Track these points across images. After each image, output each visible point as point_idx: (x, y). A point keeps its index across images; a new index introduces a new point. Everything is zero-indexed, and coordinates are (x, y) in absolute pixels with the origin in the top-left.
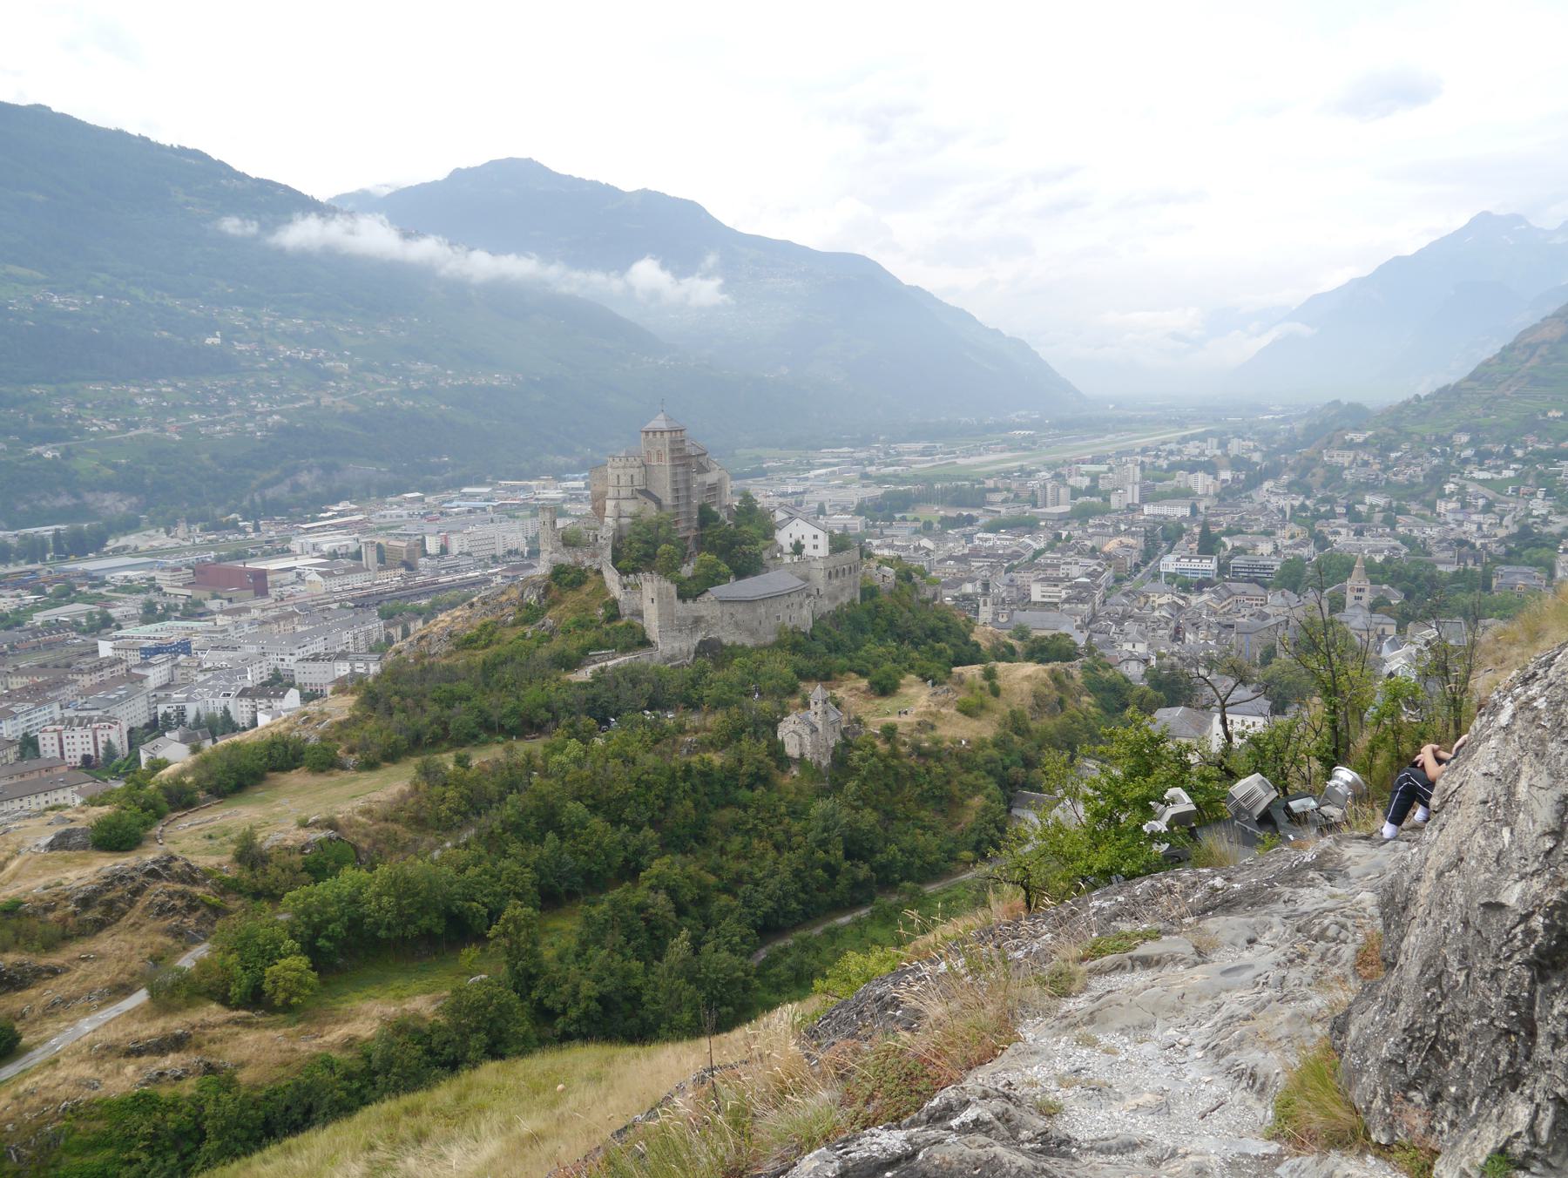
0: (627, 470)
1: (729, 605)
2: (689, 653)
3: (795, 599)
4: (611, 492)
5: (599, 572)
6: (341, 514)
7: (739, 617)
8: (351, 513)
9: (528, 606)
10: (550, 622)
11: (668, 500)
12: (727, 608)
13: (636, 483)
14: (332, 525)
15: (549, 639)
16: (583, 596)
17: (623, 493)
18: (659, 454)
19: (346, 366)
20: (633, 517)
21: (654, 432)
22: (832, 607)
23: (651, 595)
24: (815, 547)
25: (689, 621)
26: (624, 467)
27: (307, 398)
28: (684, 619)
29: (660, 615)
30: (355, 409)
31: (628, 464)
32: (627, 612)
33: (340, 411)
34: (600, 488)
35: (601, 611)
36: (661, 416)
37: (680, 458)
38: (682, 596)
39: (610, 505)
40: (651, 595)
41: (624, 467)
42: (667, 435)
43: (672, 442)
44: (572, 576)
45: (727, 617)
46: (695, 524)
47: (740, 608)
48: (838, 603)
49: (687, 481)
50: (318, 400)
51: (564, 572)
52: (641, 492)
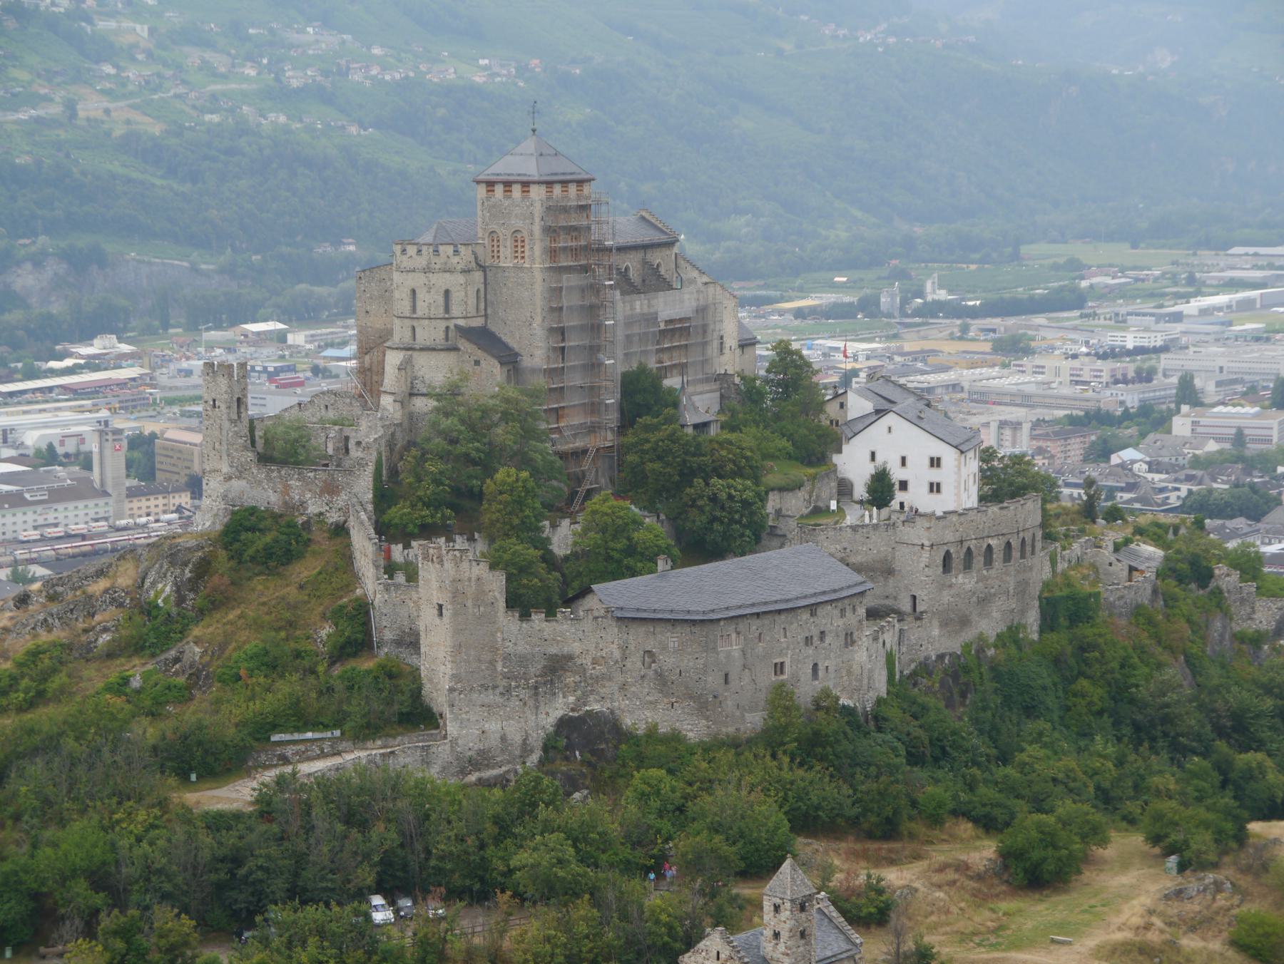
0: (434, 278)
1: (642, 630)
2: (526, 749)
3: (831, 620)
4: (400, 333)
5: (340, 531)
6: (93, 364)
7: (668, 661)
8: (120, 361)
9: (149, 610)
10: (195, 652)
11: (536, 354)
12: (639, 638)
13: (456, 310)
14: (65, 388)
15: (185, 695)
16: (292, 592)
17: (423, 337)
18: (518, 242)
19: (142, 30)
20: (439, 397)
21: (508, 185)
22: (953, 645)
23: (437, 597)
24: (935, 488)
25: (535, 668)
26: (427, 270)
27: (47, 99)
28: (523, 660)
29: (458, 648)
30: (156, 129)
31: (439, 261)
32: (388, 635)
33: (119, 131)
34: (377, 322)
35: (326, 631)
36: (530, 145)
37: (575, 252)
38: (519, 603)
39: (393, 360)
40: (437, 597)
41: (427, 270)
42: (537, 193)
43: (553, 209)
44: (268, 538)
45: (635, 662)
46: (612, 418)
47: (672, 639)
48: (969, 635)
49: (592, 310)
50: (71, 106)
51: (252, 529)
52: (468, 333)
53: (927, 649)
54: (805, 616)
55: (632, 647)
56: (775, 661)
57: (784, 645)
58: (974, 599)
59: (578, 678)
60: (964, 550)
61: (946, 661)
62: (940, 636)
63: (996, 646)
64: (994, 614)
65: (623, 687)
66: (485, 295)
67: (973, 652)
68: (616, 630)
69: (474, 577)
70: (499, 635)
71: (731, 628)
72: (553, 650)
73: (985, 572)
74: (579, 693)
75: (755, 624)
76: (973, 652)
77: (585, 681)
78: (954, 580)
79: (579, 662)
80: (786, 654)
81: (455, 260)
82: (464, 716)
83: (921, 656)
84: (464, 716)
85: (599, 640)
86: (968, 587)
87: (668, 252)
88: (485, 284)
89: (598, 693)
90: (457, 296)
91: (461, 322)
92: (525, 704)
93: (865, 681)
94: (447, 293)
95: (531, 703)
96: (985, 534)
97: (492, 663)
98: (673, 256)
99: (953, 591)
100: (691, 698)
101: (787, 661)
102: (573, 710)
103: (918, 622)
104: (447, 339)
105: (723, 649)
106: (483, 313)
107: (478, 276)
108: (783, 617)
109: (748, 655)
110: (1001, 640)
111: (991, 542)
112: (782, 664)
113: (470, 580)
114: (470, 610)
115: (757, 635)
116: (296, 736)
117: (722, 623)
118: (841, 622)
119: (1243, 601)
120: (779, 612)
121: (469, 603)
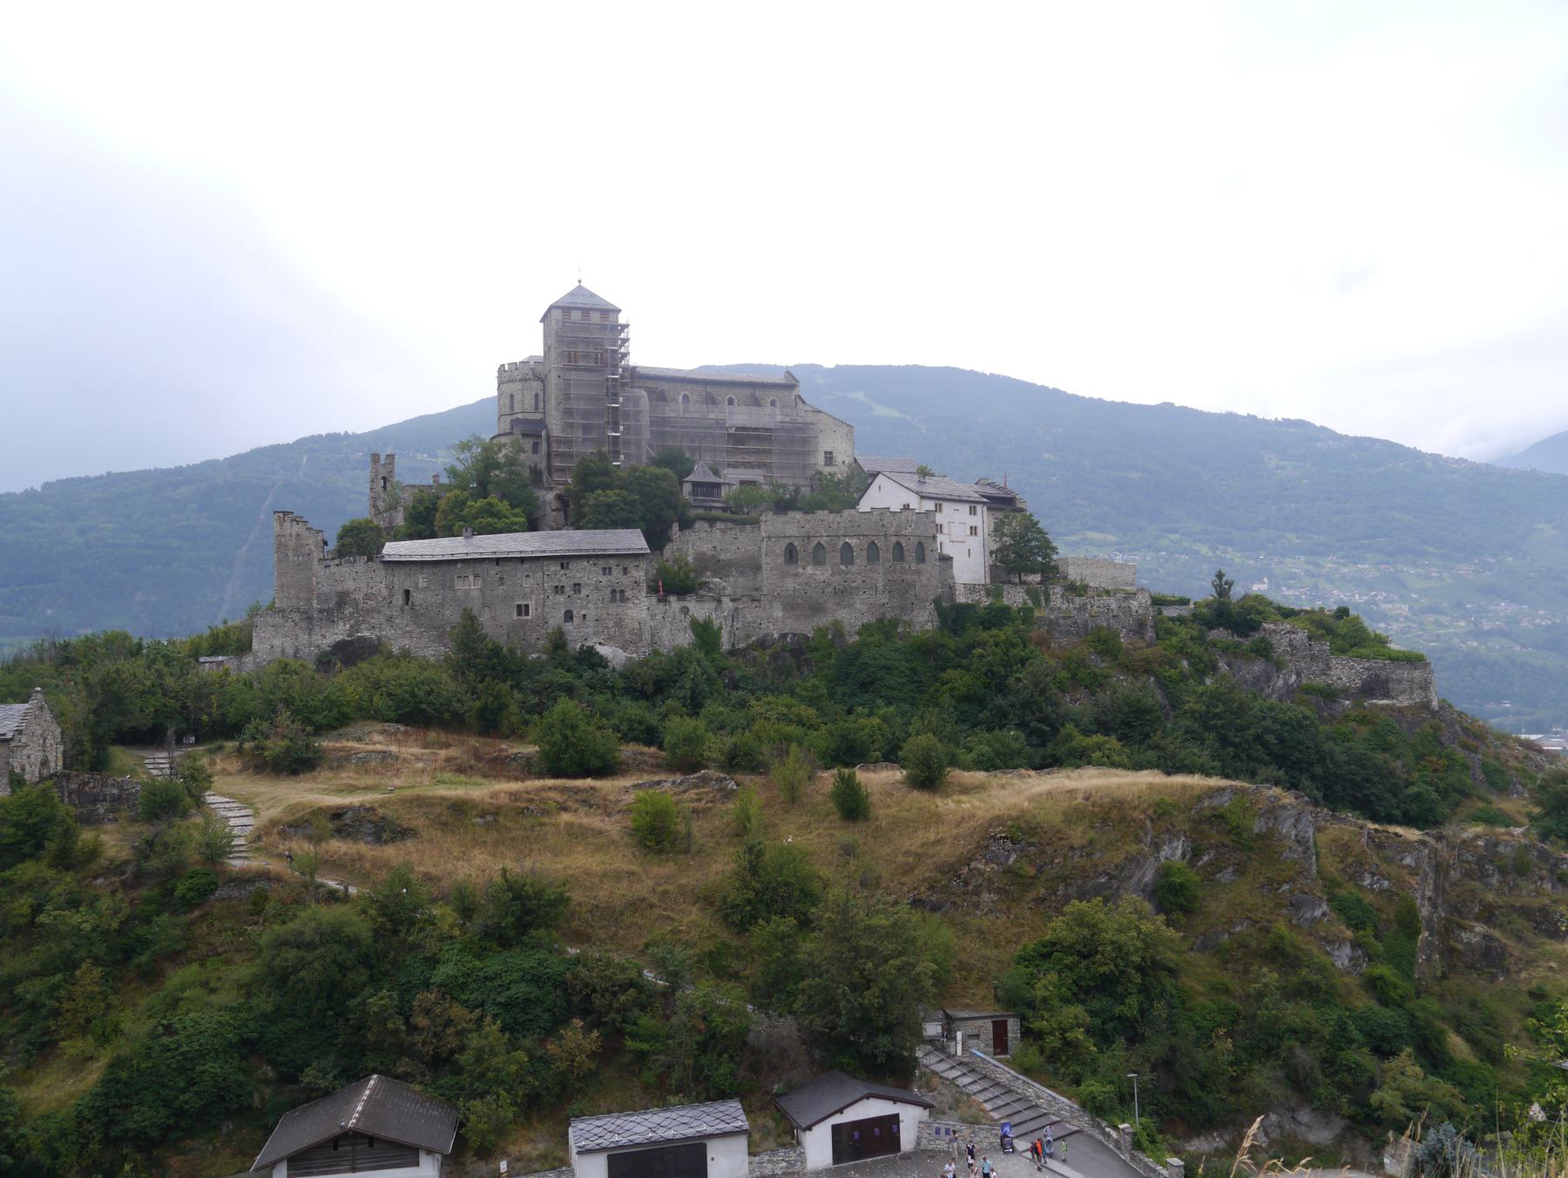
12: (401, 581)
13: (516, 410)
19: (1405, 608)
45: (399, 599)
48: (824, 621)
53: (768, 627)
54: (554, 568)
55: (396, 587)
59: (351, 610)
60: (813, 545)
63: (859, 633)
64: (858, 606)
65: (390, 619)
67: (830, 637)
69: (294, 534)
71: (469, 571)
72: (339, 588)
73: (843, 567)
74: (352, 621)
75: (494, 570)
76: (830, 637)
77: (358, 613)
78: (801, 570)
80: (531, 598)
81: (517, 372)
83: (762, 633)
85: (370, 580)
88: (544, 390)
90: (517, 398)
91: (520, 416)
93: (647, 636)
94: (512, 396)
96: (842, 532)
97: (309, 600)
98: (793, 397)
100: (435, 628)
102: (348, 636)
103: (755, 603)
104: (512, 428)
105: (459, 585)
107: (536, 385)
108: (526, 566)
110: (866, 628)
112: (527, 606)
113: (291, 534)
116: (213, 659)
117: (459, 566)
118: (604, 579)
119: (1313, 658)
120: (522, 560)
121: (290, 553)
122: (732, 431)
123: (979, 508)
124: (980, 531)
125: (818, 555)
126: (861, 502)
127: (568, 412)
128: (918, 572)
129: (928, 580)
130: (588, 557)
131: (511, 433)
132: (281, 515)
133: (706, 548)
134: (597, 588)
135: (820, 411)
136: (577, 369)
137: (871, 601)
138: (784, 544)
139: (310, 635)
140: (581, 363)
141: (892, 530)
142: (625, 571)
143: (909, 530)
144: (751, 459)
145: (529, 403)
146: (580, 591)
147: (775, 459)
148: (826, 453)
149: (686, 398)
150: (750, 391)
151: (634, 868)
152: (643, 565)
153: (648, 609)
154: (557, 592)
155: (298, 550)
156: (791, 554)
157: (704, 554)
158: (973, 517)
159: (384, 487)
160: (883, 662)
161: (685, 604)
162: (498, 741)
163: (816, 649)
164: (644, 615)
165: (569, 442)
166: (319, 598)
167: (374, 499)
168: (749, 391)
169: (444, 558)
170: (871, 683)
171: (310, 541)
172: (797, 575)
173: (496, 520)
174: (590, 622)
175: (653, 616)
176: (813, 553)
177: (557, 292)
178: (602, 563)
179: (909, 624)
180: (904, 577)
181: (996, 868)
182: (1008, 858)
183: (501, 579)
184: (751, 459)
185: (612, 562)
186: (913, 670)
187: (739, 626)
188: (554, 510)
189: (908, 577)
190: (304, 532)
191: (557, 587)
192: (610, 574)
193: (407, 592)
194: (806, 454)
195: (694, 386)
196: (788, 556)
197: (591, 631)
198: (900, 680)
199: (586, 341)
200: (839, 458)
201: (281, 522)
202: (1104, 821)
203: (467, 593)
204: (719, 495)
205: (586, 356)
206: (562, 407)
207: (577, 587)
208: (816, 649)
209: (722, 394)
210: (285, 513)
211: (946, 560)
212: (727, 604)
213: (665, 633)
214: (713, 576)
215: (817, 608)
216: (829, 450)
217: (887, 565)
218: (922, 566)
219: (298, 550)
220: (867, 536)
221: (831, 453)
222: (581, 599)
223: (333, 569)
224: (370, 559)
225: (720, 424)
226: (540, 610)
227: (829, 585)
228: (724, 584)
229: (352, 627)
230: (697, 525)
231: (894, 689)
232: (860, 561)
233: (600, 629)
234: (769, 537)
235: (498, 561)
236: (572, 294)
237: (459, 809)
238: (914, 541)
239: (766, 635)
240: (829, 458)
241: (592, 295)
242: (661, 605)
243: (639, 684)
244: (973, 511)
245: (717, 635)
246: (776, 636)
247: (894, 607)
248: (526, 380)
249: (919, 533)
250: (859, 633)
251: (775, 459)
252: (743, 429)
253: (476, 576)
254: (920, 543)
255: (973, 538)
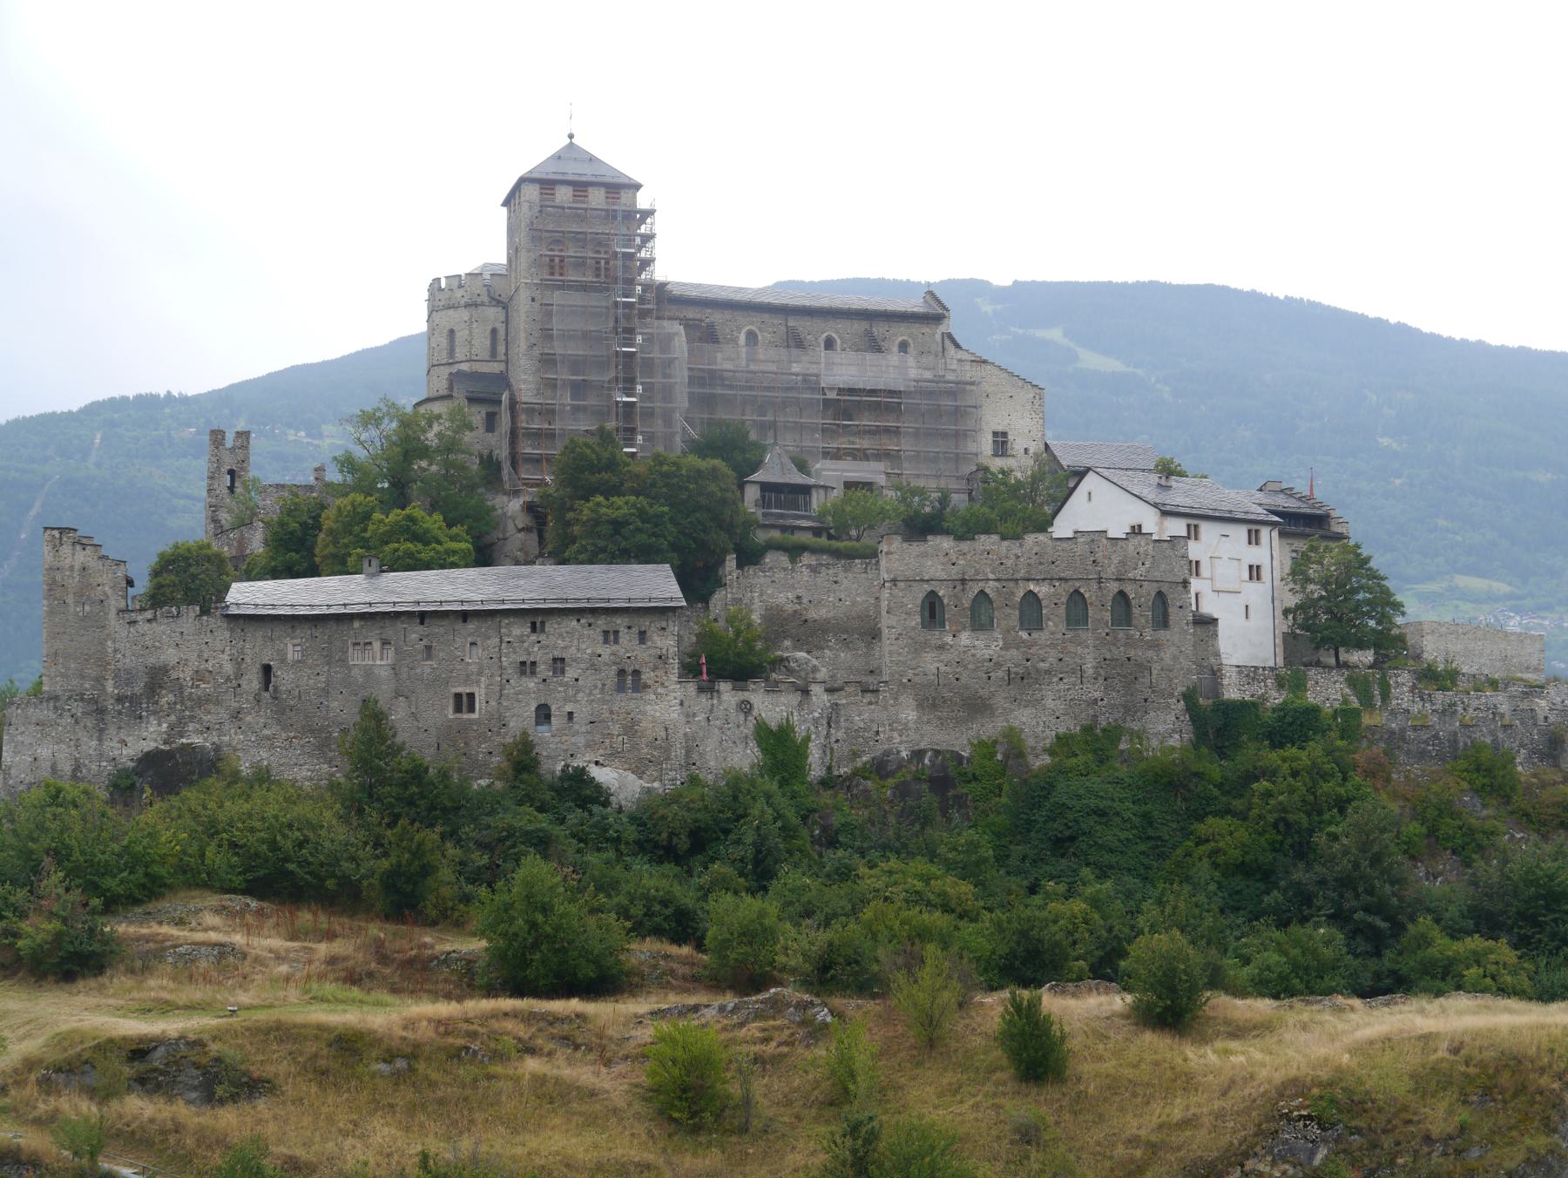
12: (257, 648)
13: (459, 356)
45: (252, 681)
48: (989, 728)
53: (890, 739)
54: (519, 629)
56: (459, 690)
57: (473, 668)
58: (1000, 674)
59: (171, 698)
60: (971, 595)
61: (926, 761)
62: (919, 721)
63: (1051, 752)
64: (1049, 703)
65: (236, 715)
66: (506, 340)
67: (999, 757)
68: (227, 634)
70: (109, 643)
71: (373, 634)
72: (152, 661)
73: (1024, 635)
74: (173, 718)
75: (415, 632)
76: (999, 757)
77: (182, 703)
78: (949, 639)
79: (174, 675)
80: (478, 682)
81: (459, 293)
82: (19, 738)
83: (880, 749)
84: (19, 738)
85: (204, 646)
86: (987, 653)
87: (926, 330)
88: (507, 322)
89: (200, 721)
90: (461, 335)
91: (465, 367)
92: (77, 722)
93: (678, 752)
94: (452, 332)
95: (90, 722)
96: (1022, 574)
97: (99, 680)
98: (938, 337)
99: (945, 657)
100: (312, 731)
101: (480, 694)
102: (165, 743)
103: (869, 697)
104: (451, 388)
105: (356, 658)
106: (503, 358)
107: (493, 314)
108: (471, 626)
109: (404, 676)
110: (1063, 743)
111: (1032, 587)
112: (471, 696)
113: (72, 568)
114: (72, 609)
115: (420, 646)
117: (356, 624)
118: (606, 651)
120: (465, 616)
121: (70, 600)
122: (832, 395)
123: (1265, 532)
124: (1266, 573)
125: (980, 614)
126: (1058, 521)
127: (548, 361)
128: (1156, 645)
129: (1175, 658)
130: (578, 613)
131: (449, 397)
132: (56, 533)
133: (784, 599)
134: (594, 667)
135: (985, 362)
136: (564, 286)
137: (1072, 694)
138: (920, 592)
139: (100, 740)
140: (572, 276)
141: (1111, 571)
142: (642, 636)
143: (1141, 570)
144: (864, 443)
145: (481, 344)
146: (563, 672)
147: (906, 445)
148: (995, 434)
149: (751, 336)
150: (864, 325)
151: (650, 1157)
152: (674, 628)
153: (682, 704)
154: (523, 673)
155: (82, 596)
156: (932, 610)
157: (779, 609)
158: (1254, 549)
159: (231, 489)
160: (1093, 802)
161: (746, 695)
162: (417, 930)
163: (975, 778)
164: (675, 714)
165: (549, 413)
166: (116, 676)
167: (214, 508)
168: (859, 327)
169: (332, 611)
170: (1072, 839)
171: (104, 579)
172: (942, 647)
173: (420, 546)
174: (580, 725)
175: (689, 717)
176: (972, 609)
177: (532, 155)
178: (602, 623)
179: (1139, 736)
180: (1132, 653)
181: (1291, 1171)
182: (1312, 1154)
183: (429, 648)
184: (864, 443)
185: (620, 622)
186: (1146, 816)
187: (840, 735)
188: (520, 531)
189: (1137, 654)
190: (93, 564)
191: (523, 663)
192: (616, 641)
193: (267, 670)
194: (960, 436)
195: (766, 317)
196: (927, 614)
197: (581, 740)
198: (1123, 835)
199: (581, 239)
200: (1018, 443)
201: (56, 546)
202: (1487, 1092)
203: (368, 672)
204: (807, 505)
205: (580, 264)
206: (537, 352)
207: (559, 664)
208: (975, 778)
209: (816, 331)
210: (62, 530)
211: (1207, 623)
212: (820, 697)
213: (710, 747)
214: (795, 648)
215: (977, 707)
216: (1000, 428)
217: (1102, 632)
218: (1163, 634)
219: (82, 596)
220: (1066, 580)
221: (1004, 434)
222: (566, 685)
223: (143, 627)
224: (205, 611)
225: (811, 383)
226: (493, 703)
227: (999, 665)
228: (815, 662)
229: (171, 727)
230: (769, 559)
231: (1111, 851)
232: (1054, 624)
233: (598, 738)
234: (894, 581)
235: (423, 617)
236: (558, 157)
237: (349, 1045)
238: (1150, 590)
239: (887, 753)
240: (1001, 442)
241: (592, 159)
242: (703, 699)
243: (664, 835)
244: (1254, 538)
245: (801, 751)
246: (904, 754)
247: (1113, 706)
248: (476, 305)
249: (1157, 575)
250: (1051, 752)
251: (906, 445)
252: (852, 391)
253: (385, 642)
254: (1160, 594)
255: (1254, 585)
